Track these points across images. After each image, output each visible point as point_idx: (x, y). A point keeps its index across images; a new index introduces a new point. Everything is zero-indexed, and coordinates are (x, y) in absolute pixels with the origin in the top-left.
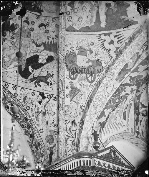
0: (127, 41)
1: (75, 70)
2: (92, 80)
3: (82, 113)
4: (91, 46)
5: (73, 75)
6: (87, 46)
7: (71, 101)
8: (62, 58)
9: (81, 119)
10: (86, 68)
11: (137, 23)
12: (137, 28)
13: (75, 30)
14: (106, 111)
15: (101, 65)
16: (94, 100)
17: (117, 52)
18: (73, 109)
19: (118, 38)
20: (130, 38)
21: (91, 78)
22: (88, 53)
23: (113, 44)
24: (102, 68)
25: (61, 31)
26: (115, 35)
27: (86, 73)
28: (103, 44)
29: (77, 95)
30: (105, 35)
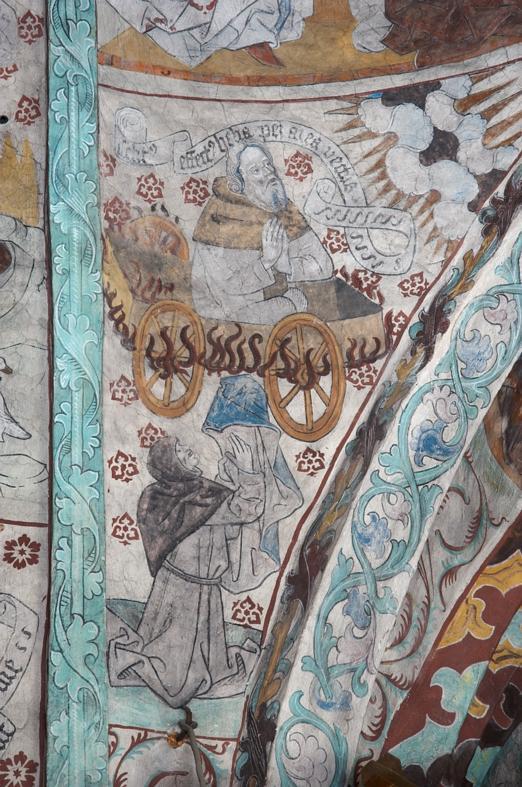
1: (178, 345)
2: (315, 418)
3: (252, 663)
4: (286, 180)
5: (161, 376)
6: (261, 182)
7: (154, 574)
8: (75, 231)
9: (248, 713)
10: (265, 337)
13: (170, 65)
14: (443, 677)
15: (378, 308)
16: (345, 544)
17: (487, 204)
18: (173, 633)
19: (486, 116)
21: (308, 404)
22: (269, 232)
23: (453, 157)
25: (61, 33)
26: (462, 95)
27: (267, 366)
28: (380, 164)
29: (202, 522)
30: (391, 98)
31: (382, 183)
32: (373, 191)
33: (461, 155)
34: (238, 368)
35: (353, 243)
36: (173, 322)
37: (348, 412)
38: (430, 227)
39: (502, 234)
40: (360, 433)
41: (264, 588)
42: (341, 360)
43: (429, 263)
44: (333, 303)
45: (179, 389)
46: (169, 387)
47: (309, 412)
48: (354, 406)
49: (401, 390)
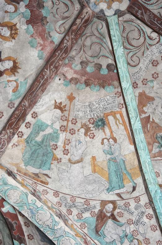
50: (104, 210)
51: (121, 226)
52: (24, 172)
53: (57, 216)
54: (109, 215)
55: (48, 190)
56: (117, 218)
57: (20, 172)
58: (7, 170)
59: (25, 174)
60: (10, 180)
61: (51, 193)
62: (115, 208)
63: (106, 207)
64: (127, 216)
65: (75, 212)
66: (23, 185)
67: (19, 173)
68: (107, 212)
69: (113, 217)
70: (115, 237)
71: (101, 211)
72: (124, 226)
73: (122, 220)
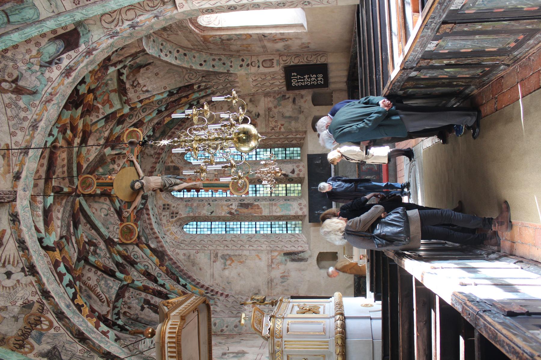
0: (21, 253)
3: (92, 354)
11: (4, 231)
12: (11, 234)
15: (34, 302)
19: (9, 263)
20: (19, 247)
21: (45, 324)
23: (13, 273)
24: (39, 302)
29: (59, 353)
31: (8, 289)
32: (8, 291)
33: (13, 272)
34: (29, 333)
35: (16, 300)
36: (12, 341)
37: (51, 318)
38: (24, 285)
39: (38, 273)
40: (57, 318)
41: (78, 347)
42: (40, 314)
43: (31, 289)
44: (26, 310)
45: (28, 346)
46: (27, 348)
47: (47, 325)
48: (51, 316)
49: (57, 305)
50: (11, 89)
51: (22, 74)
52: (7, 167)
53: (37, 130)
54: (14, 85)
55: (13, 142)
56: (15, 77)
57: (10, 170)
58: (15, 181)
59: (9, 165)
60: (23, 175)
61: (14, 139)
62: (6, 81)
63: (6, 88)
64: (9, 70)
65: (22, 114)
66: (22, 164)
67: (11, 171)
68: (12, 87)
69: (15, 81)
70: (33, 78)
71: (13, 92)
72: (21, 71)
73: (16, 74)
